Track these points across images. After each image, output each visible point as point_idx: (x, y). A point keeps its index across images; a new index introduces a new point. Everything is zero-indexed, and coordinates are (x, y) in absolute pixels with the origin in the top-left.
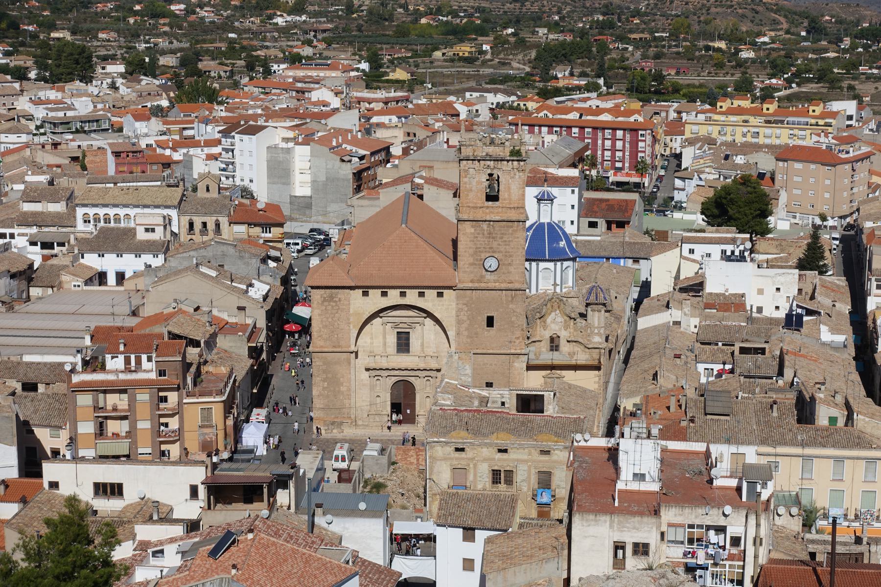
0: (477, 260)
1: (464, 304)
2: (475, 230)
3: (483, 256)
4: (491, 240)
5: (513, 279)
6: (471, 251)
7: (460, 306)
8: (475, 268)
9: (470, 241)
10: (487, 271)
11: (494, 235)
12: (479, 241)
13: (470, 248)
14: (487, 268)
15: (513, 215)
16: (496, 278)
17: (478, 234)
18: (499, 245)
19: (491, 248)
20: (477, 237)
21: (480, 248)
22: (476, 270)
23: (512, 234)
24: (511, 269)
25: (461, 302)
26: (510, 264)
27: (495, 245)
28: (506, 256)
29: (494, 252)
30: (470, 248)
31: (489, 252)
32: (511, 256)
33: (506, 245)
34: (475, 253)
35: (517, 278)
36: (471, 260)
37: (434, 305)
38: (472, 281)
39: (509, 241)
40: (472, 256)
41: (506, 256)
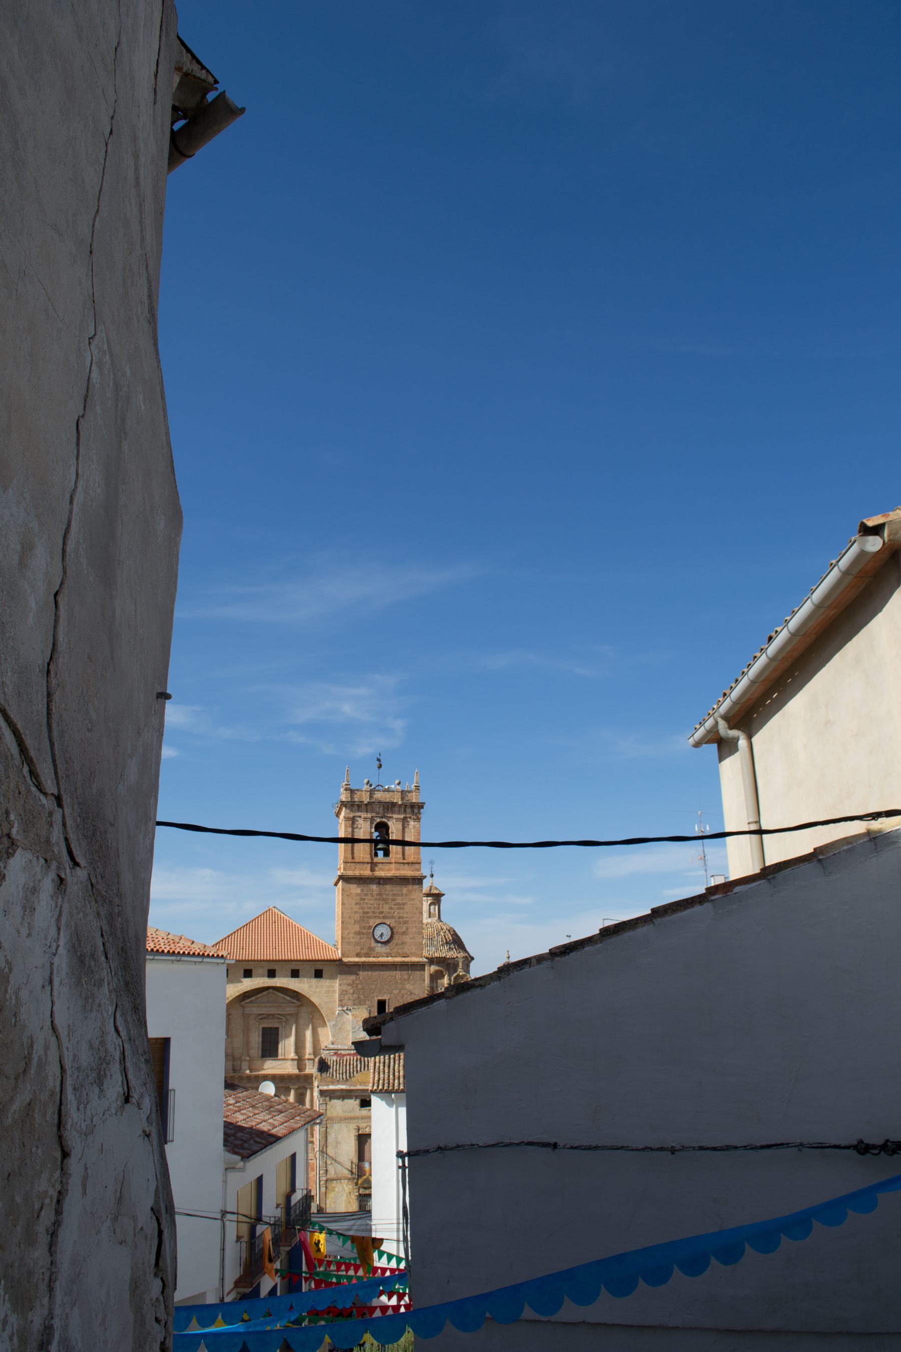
0: (364, 927)
1: (349, 985)
2: (362, 890)
3: (373, 922)
4: (382, 903)
5: (408, 952)
6: (357, 916)
7: (344, 987)
8: (361, 938)
9: (357, 904)
10: (377, 942)
11: (384, 897)
12: (367, 904)
13: (356, 912)
14: (376, 937)
15: (407, 872)
16: (388, 951)
17: (366, 895)
18: (391, 908)
19: (382, 913)
20: (364, 899)
21: (367, 913)
22: (362, 940)
23: (406, 895)
24: (407, 939)
25: (345, 982)
26: (404, 933)
27: (386, 908)
28: (400, 923)
29: (384, 918)
30: (356, 912)
31: (379, 918)
32: (406, 922)
33: (399, 908)
34: (362, 919)
35: (414, 951)
36: (357, 928)
37: (310, 987)
38: (358, 955)
39: (404, 904)
40: (359, 922)
41: (400, 923)
